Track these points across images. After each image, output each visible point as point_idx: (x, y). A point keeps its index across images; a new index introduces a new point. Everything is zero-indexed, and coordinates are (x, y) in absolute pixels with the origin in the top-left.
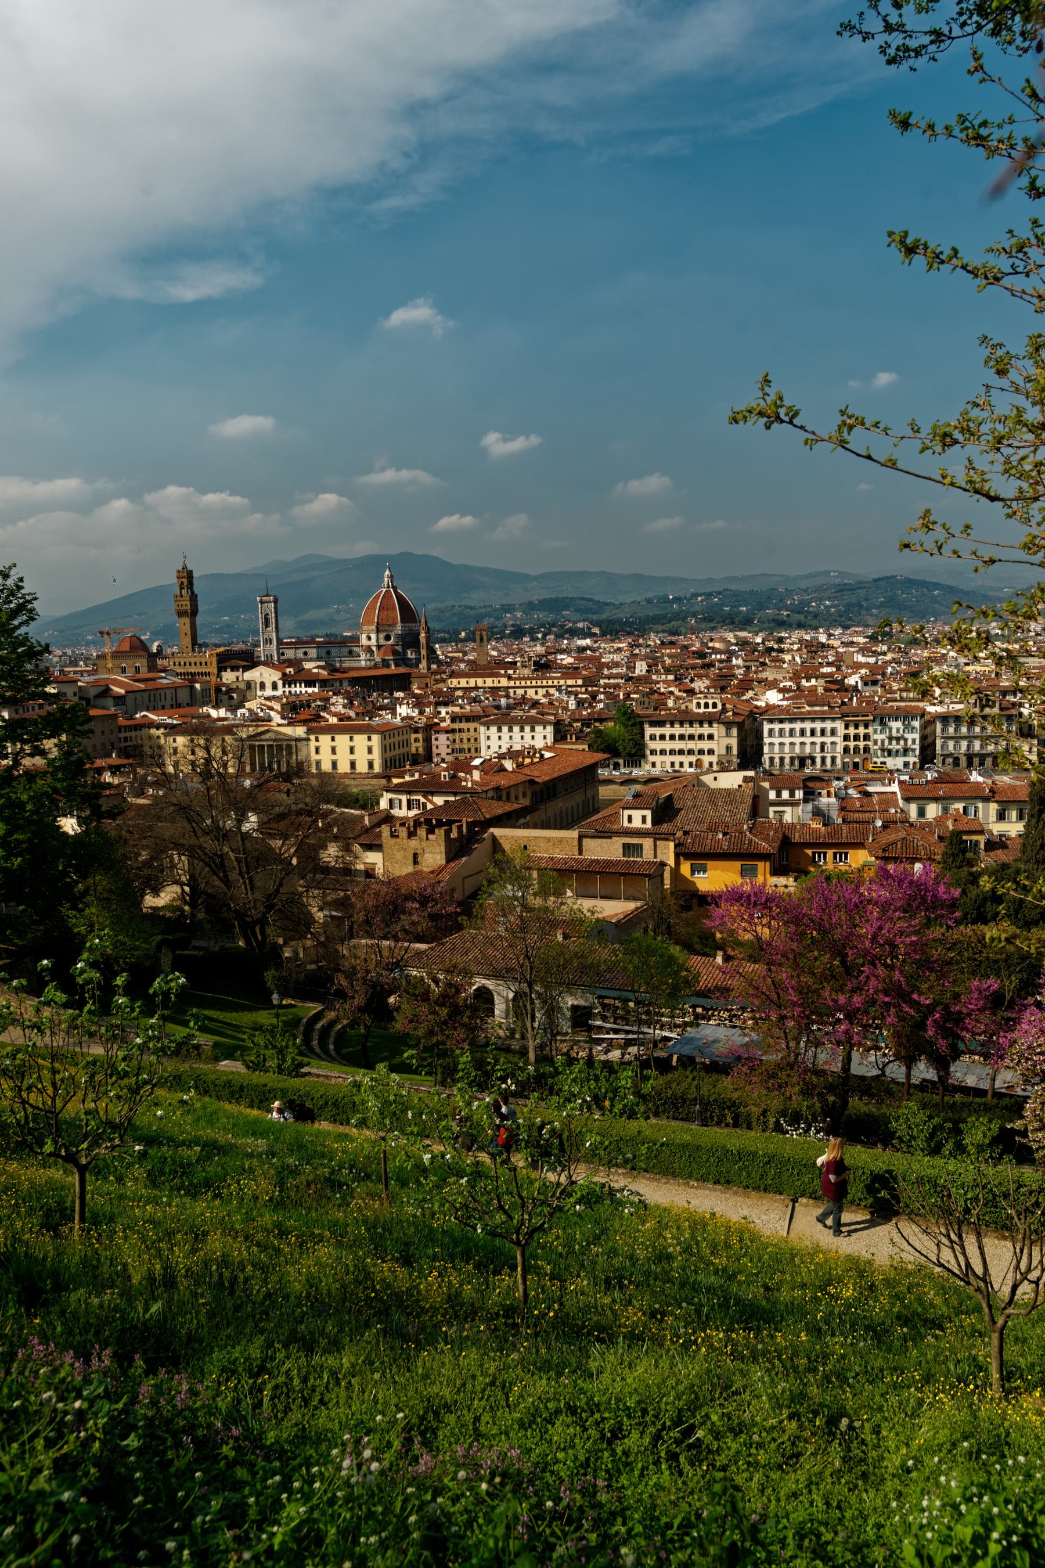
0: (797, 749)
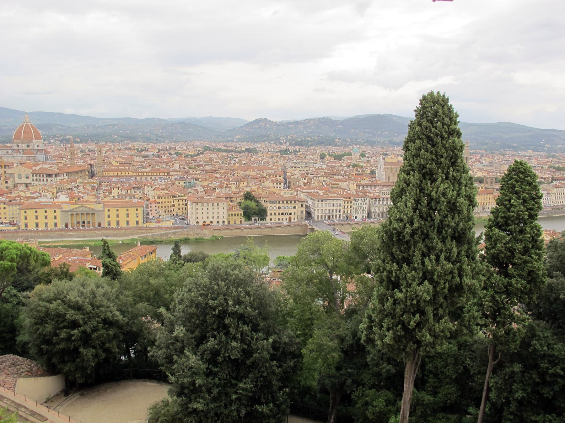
0: (327, 212)
